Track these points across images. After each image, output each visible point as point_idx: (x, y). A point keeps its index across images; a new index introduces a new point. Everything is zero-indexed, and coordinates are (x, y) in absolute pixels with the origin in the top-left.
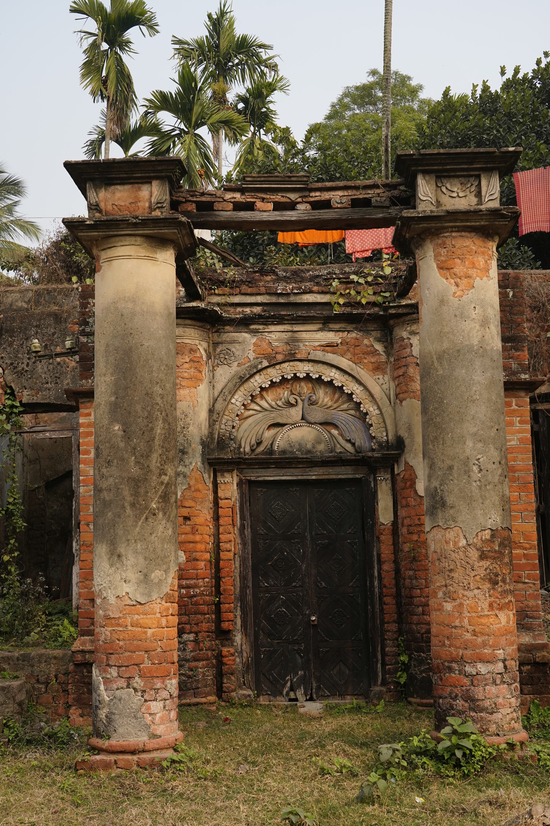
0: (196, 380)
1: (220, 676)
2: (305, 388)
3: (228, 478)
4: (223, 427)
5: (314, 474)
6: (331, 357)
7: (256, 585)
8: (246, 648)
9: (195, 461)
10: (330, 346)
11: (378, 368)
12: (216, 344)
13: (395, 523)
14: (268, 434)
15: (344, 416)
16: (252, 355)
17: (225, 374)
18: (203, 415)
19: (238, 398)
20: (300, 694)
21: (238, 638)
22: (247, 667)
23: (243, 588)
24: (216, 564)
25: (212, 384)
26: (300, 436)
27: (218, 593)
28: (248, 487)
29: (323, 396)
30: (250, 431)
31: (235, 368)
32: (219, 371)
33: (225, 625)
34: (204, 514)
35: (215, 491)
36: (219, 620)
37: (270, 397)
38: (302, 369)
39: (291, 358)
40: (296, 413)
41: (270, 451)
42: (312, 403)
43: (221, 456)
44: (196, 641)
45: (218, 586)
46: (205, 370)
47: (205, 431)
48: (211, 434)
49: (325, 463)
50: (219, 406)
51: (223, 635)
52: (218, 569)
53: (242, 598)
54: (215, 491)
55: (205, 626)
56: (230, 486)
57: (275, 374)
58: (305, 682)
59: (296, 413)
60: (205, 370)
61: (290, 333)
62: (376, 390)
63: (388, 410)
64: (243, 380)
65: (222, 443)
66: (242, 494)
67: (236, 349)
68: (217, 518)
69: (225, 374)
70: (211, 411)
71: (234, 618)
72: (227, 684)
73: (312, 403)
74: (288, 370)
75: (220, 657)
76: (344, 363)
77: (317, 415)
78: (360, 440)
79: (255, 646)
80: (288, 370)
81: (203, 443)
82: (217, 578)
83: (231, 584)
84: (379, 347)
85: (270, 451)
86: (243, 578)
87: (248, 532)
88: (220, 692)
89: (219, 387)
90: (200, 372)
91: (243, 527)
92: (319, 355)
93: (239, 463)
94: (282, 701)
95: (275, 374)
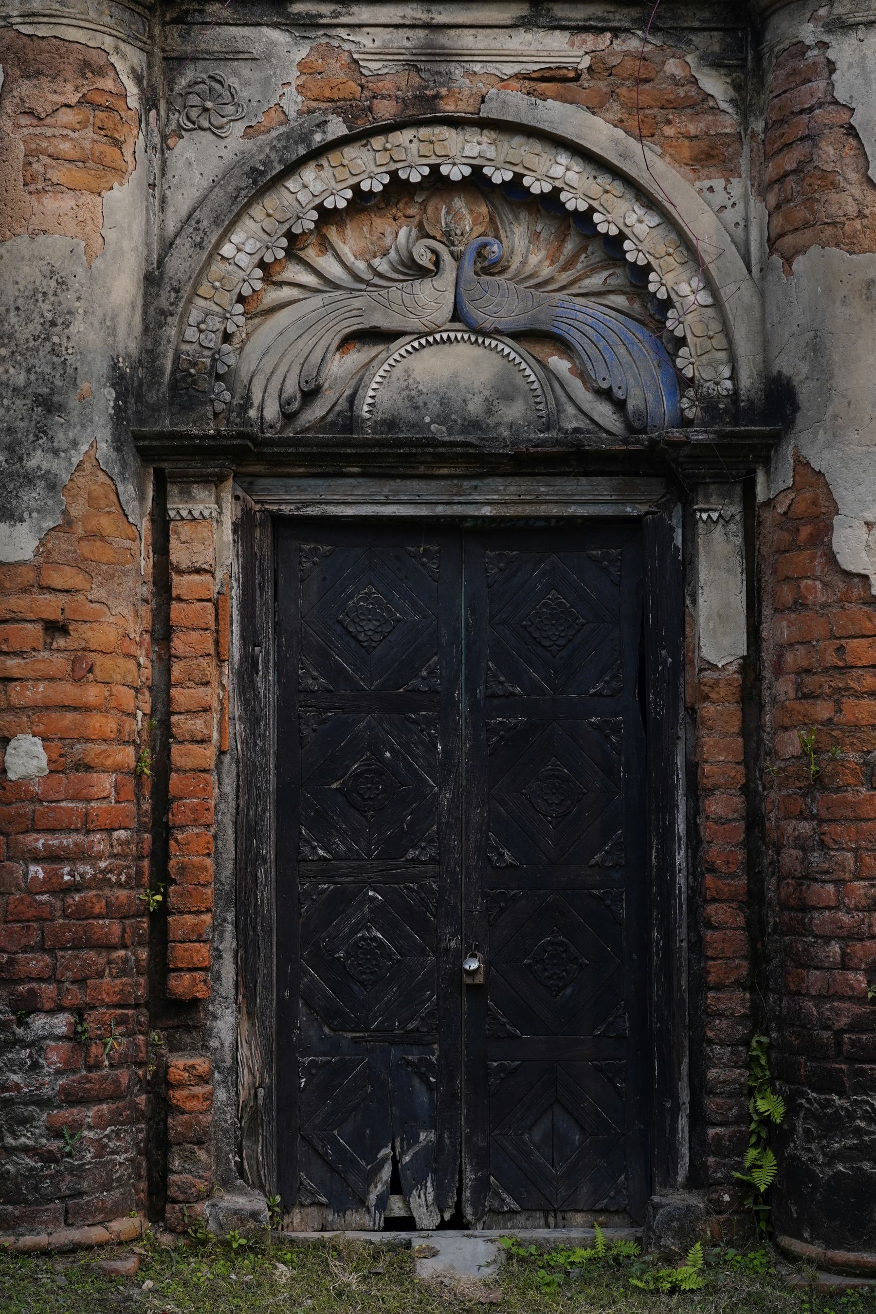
0: (104, 169)
1: (159, 1147)
2: (466, 217)
3: (203, 502)
4: (192, 334)
5: (489, 499)
6: (555, 114)
7: (289, 855)
8: (250, 1056)
9: (91, 436)
10: (552, 79)
11: (708, 156)
12: (175, 63)
13: (750, 664)
14: (342, 366)
15: (593, 312)
16: (293, 102)
17: (201, 162)
18: (123, 288)
19: (245, 244)
20: (422, 1204)
21: (225, 1024)
22: (251, 1118)
23: (247, 861)
24: (158, 785)
25: (157, 188)
26: (446, 373)
27: (162, 877)
28: (272, 538)
29: (524, 245)
30: (281, 354)
31: (235, 142)
32: (184, 150)
33: (181, 984)
34: (117, 617)
35: (161, 548)
36: (161, 967)
37: (349, 243)
38: (462, 152)
39: (422, 112)
40: (433, 298)
41: (347, 419)
42: (491, 268)
43: (179, 429)
44: (75, 1037)
45: (160, 855)
46: (136, 142)
47: (128, 340)
48: (150, 356)
49: (524, 462)
50: (179, 264)
51: (177, 1015)
52: (163, 800)
53: (241, 895)
54: (161, 548)
55: (109, 986)
56: (211, 532)
57: (367, 166)
58: (439, 1165)
59: (433, 298)
60: (136, 142)
61: (421, 33)
62: (703, 224)
63: (738, 292)
64: (261, 181)
65: (188, 386)
66: (249, 561)
67: (241, 79)
68: (162, 632)
69: (201, 162)
70: (152, 280)
71: (213, 959)
72: (180, 1176)
73: (491, 268)
74: (412, 152)
75: (160, 1086)
76: (600, 132)
77: (504, 306)
78: (643, 386)
79: (282, 1051)
80: (412, 152)
81: (117, 379)
82: (161, 829)
83: (207, 850)
84: (715, 85)
85: (347, 419)
86: (247, 830)
87: (266, 682)
88: (158, 1200)
89: (181, 203)
90: (117, 144)
91: (248, 668)
92: (515, 104)
93: (241, 455)
94: (360, 1232)
95: (367, 166)
